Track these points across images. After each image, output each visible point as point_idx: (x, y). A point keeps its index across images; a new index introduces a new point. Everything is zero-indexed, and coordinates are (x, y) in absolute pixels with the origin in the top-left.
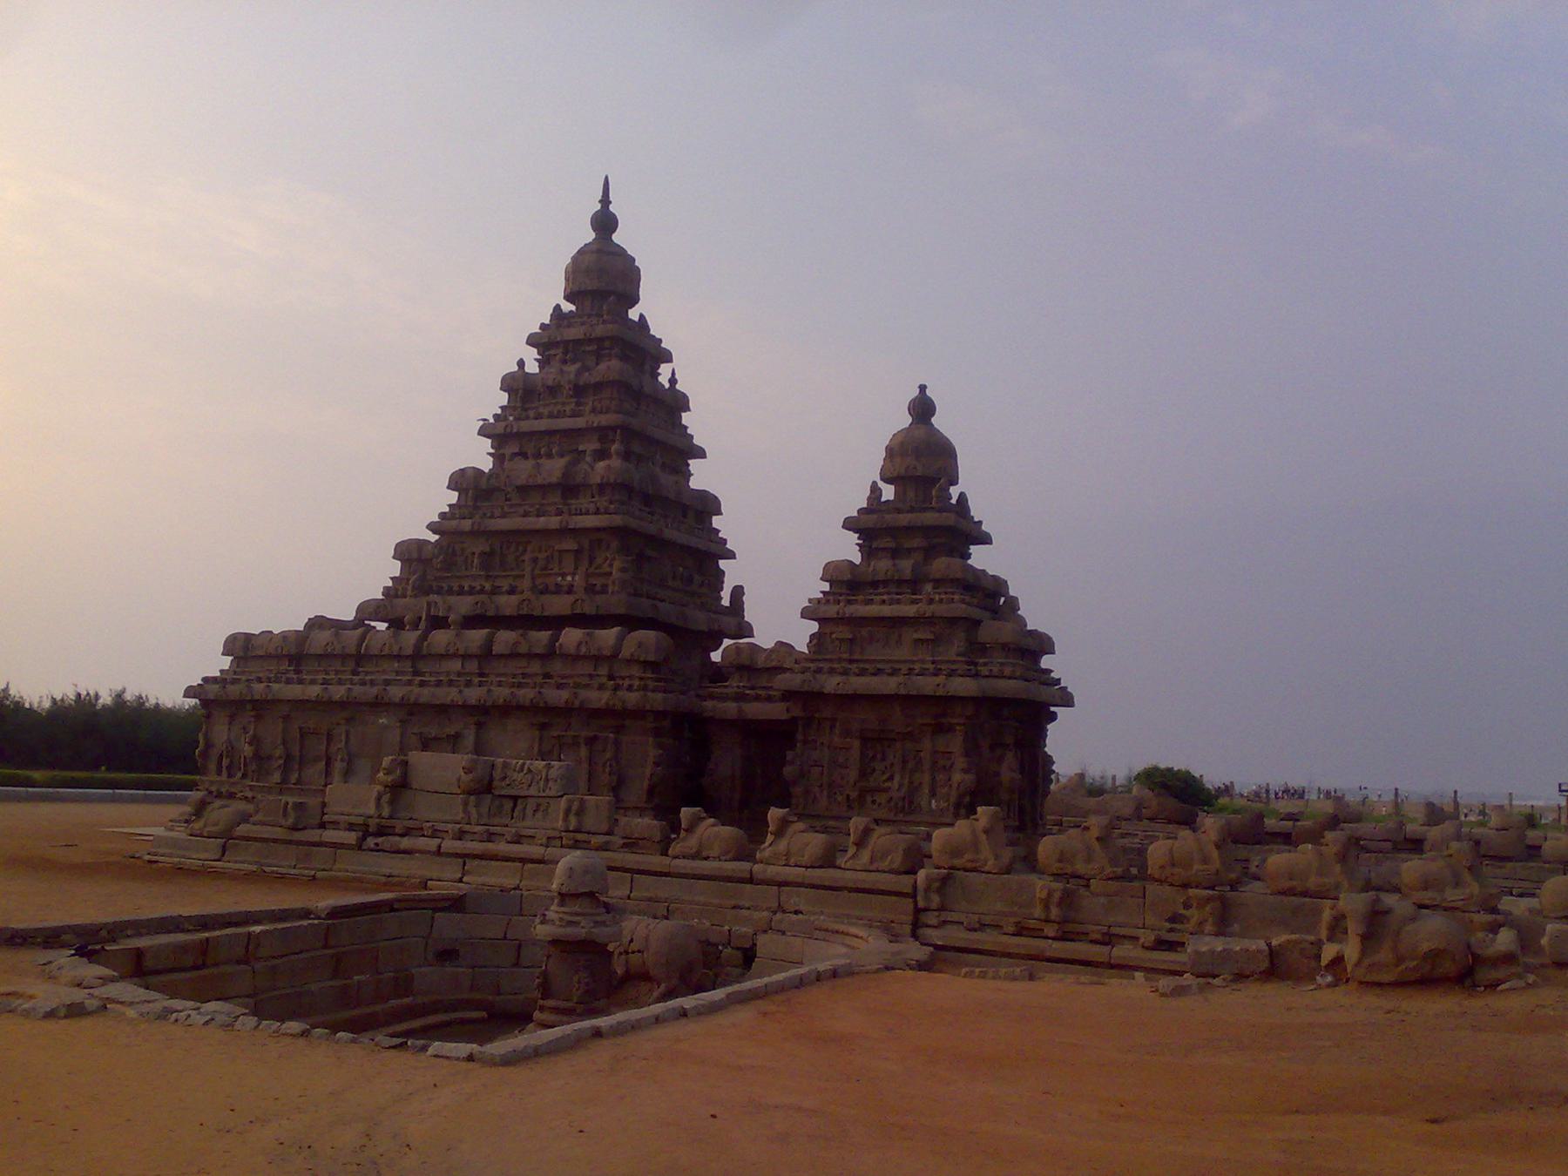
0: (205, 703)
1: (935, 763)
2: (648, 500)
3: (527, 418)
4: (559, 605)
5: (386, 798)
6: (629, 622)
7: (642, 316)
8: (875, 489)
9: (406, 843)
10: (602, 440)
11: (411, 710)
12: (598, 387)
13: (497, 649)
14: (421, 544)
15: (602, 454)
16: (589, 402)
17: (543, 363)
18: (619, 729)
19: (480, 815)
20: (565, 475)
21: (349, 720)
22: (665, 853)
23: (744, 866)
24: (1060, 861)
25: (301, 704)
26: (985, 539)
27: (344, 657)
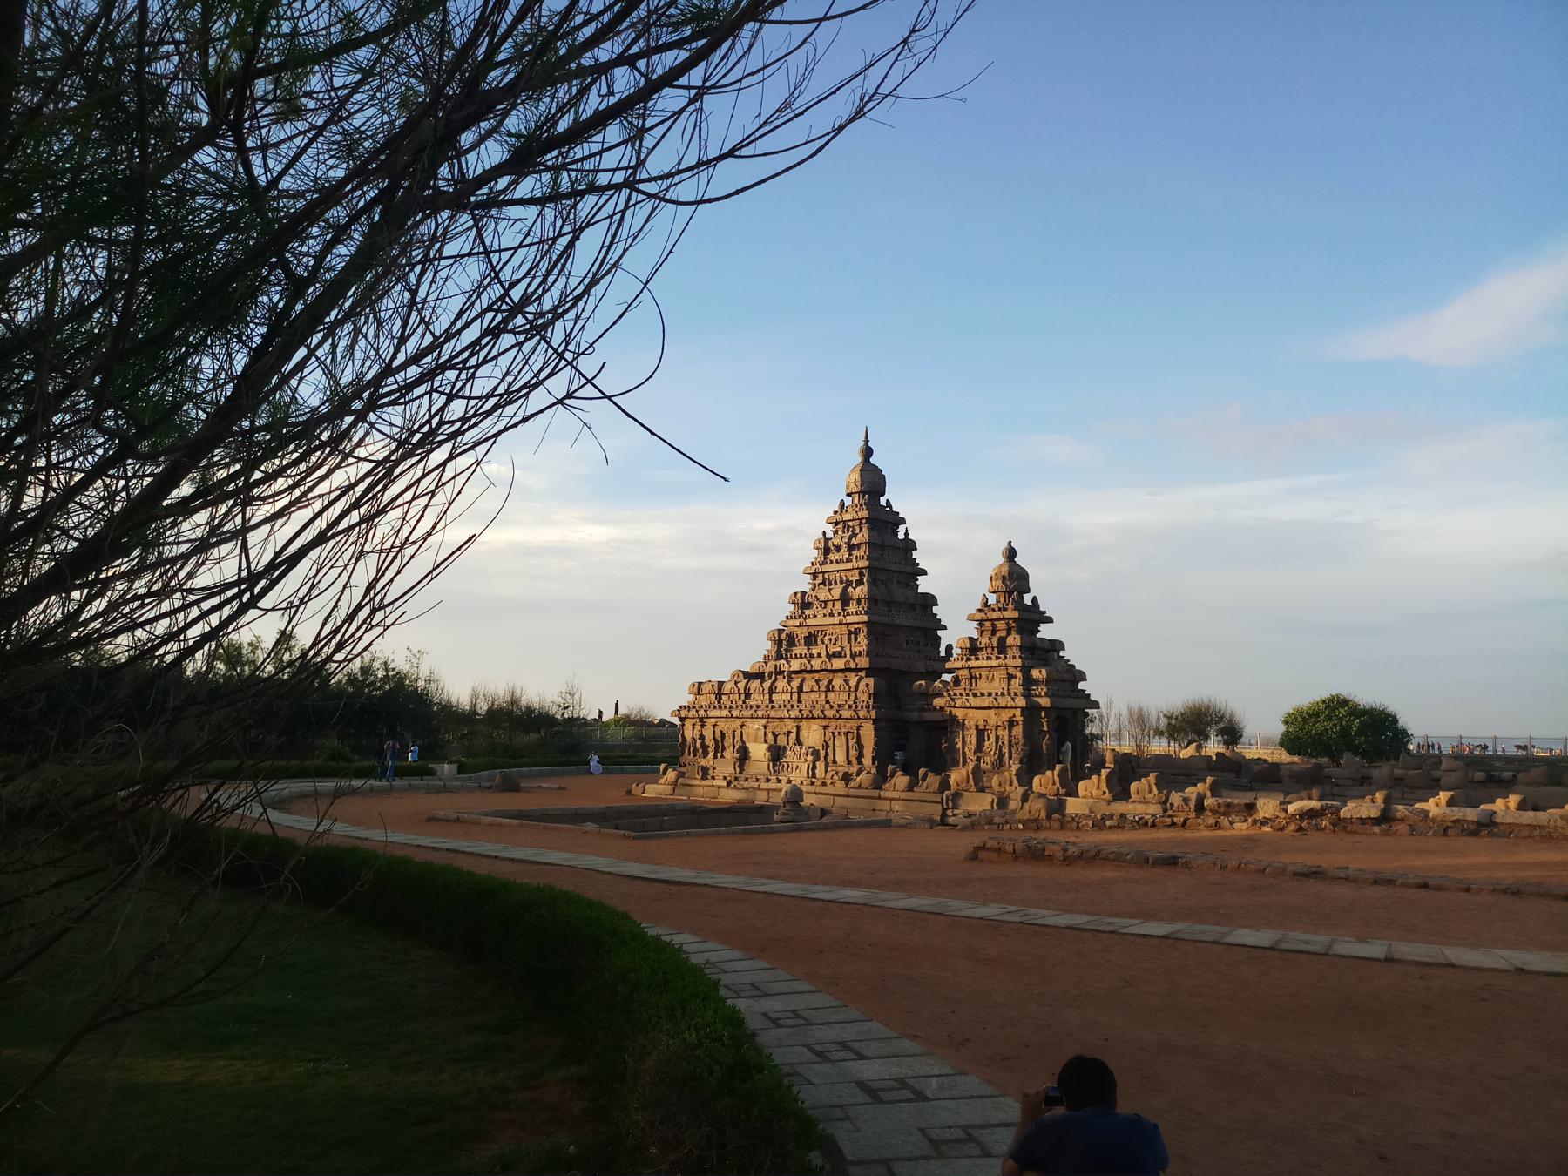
1: (1010, 742)
2: (888, 603)
3: (826, 563)
4: (838, 664)
5: (737, 764)
7: (887, 500)
8: (985, 600)
9: (746, 784)
10: (861, 574)
15: (860, 582)
16: (855, 553)
17: (836, 532)
19: (775, 771)
22: (847, 787)
23: (875, 793)
24: (1000, 785)
26: (1050, 620)
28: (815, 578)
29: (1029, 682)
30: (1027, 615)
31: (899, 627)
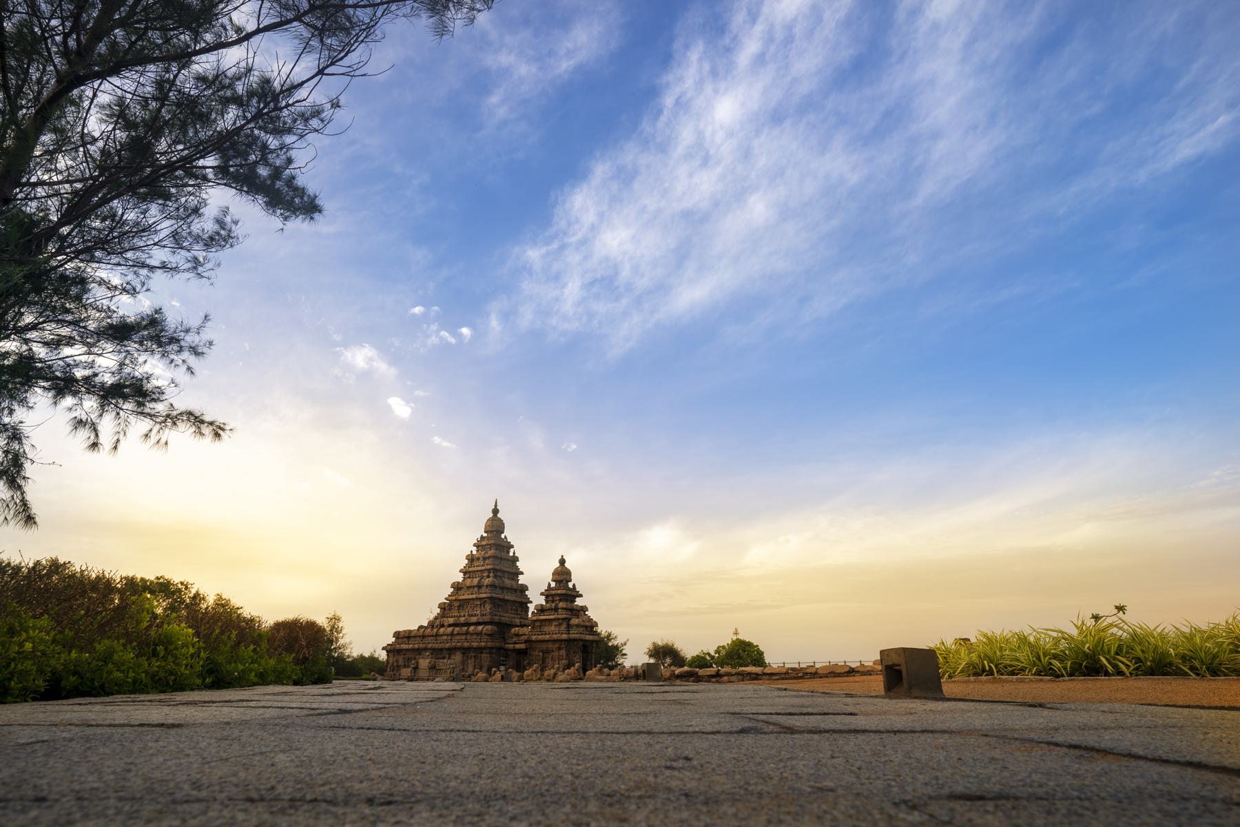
0: (387, 651)
4: (474, 619)
6: (485, 623)
8: (549, 584)
11: (434, 650)
12: (489, 558)
13: (455, 632)
14: (445, 603)
15: (488, 577)
16: (487, 561)
17: (478, 551)
18: (481, 653)
20: (479, 582)
21: (420, 654)
25: (408, 650)
27: (420, 636)
28: (465, 575)
29: (569, 626)
30: (569, 592)
31: (507, 601)
